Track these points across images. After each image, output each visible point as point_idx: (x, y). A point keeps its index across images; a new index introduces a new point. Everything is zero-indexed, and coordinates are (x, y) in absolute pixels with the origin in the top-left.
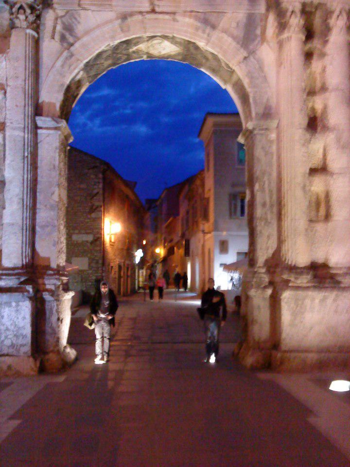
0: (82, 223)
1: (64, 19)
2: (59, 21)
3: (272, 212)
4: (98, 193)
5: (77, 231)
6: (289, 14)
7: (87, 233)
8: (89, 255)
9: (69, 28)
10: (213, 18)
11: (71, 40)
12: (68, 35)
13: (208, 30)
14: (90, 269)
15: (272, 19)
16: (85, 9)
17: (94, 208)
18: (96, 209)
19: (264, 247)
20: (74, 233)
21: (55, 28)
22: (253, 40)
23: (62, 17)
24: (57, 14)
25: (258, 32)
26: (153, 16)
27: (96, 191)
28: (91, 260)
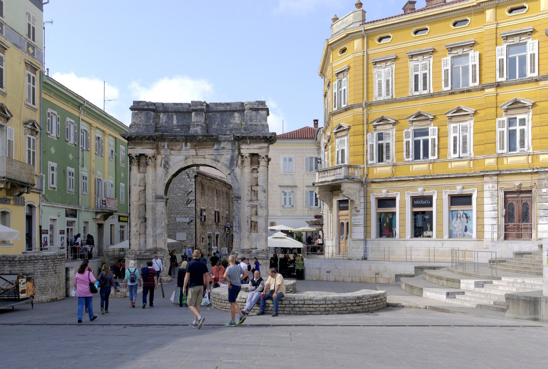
0: (182, 210)
1: (165, 159)
2: (163, 159)
3: (238, 229)
4: (192, 191)
5: (179, 216)
6: (244, 158)
7: (185, 217)
8: (187, 231)
9: (167, 163)
10: (218, 158)
11: (167, 167)
12: (166, 165)
13: (216, 162)
14: (188, 240)
15: (240, 157)
16: (172, 155)
17: (190, 200)
18: (190, 202)
19: (235, 241)
20: (177, 217)
21: (162, 161)
22: (233, 166)
23: (164, 158)
24: (162, 157)
25: (235, 162)
26: (197, 156)
27: (190, 191)
28: (188, 234)
